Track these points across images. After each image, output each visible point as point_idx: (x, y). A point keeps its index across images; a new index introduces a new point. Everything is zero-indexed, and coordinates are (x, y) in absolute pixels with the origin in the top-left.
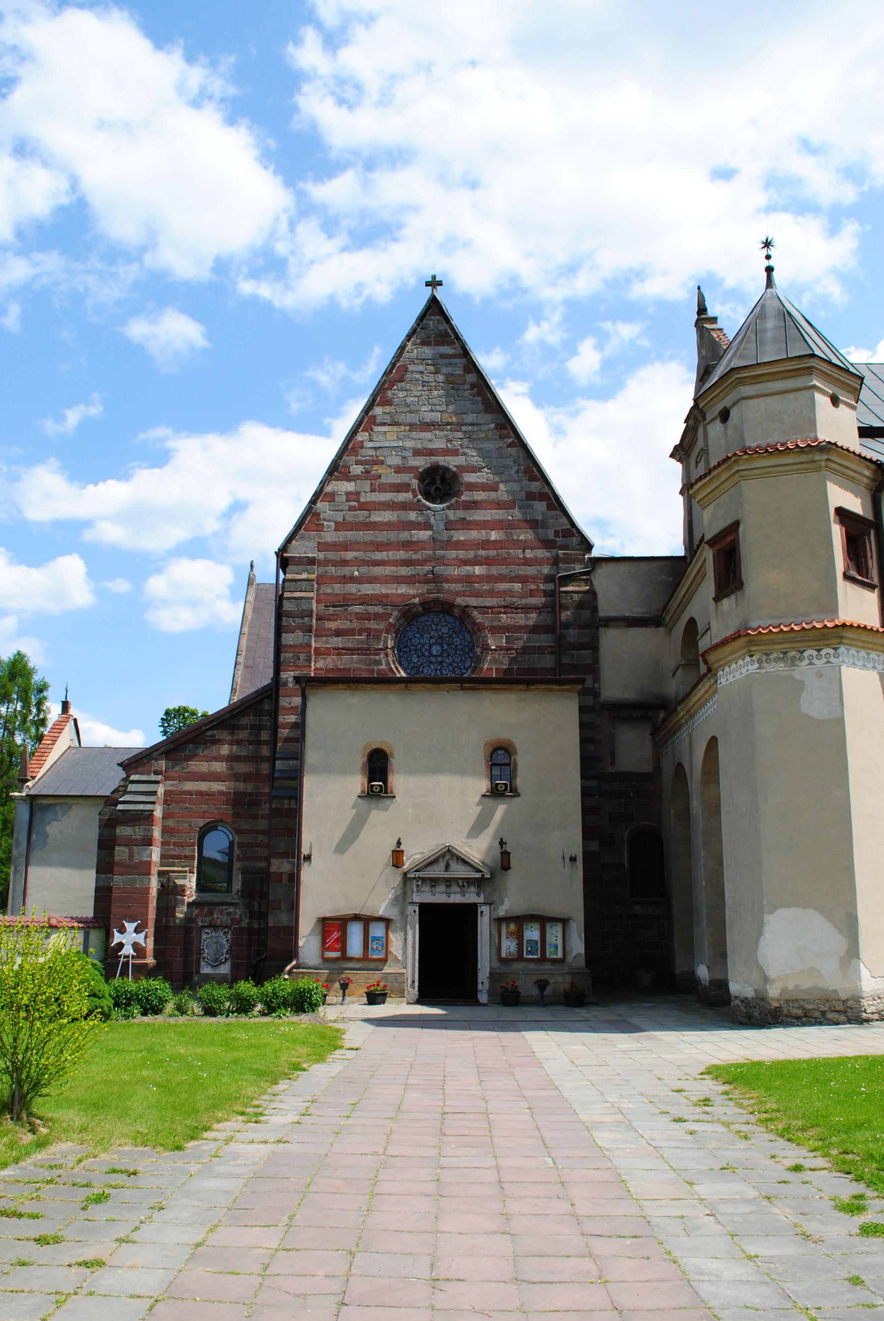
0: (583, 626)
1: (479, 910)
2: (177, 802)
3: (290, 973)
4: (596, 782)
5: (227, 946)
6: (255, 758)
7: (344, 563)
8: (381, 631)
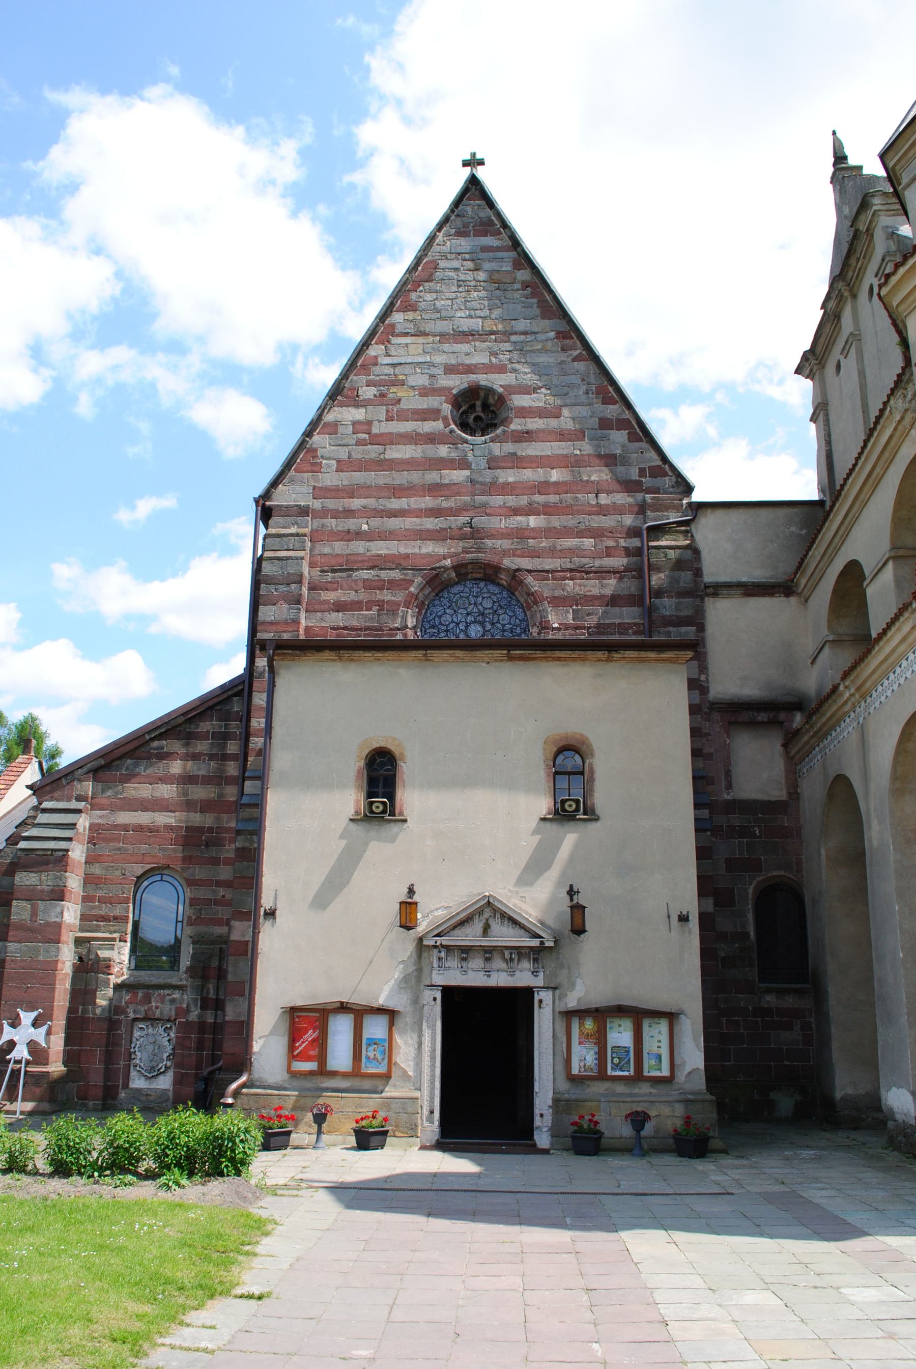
0: (681, 594)
1: (537, 998)
2: (107, 840)
3: (236, 1094)
4: (707, 811)
5: (169, 1049)
6: (219, 779)
7: (349, 513)
8: (398, 604)
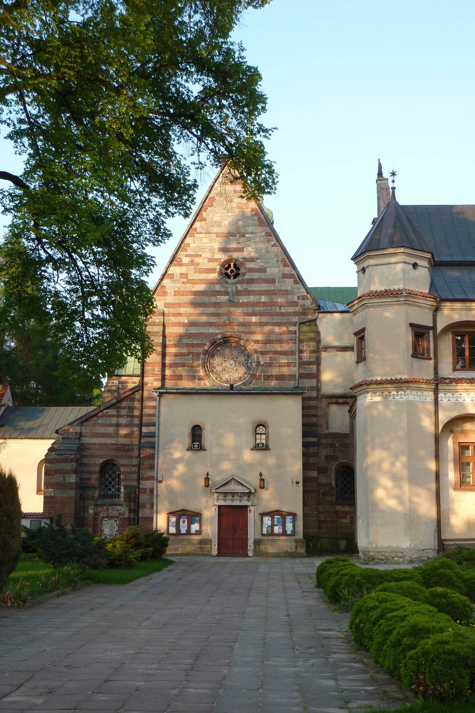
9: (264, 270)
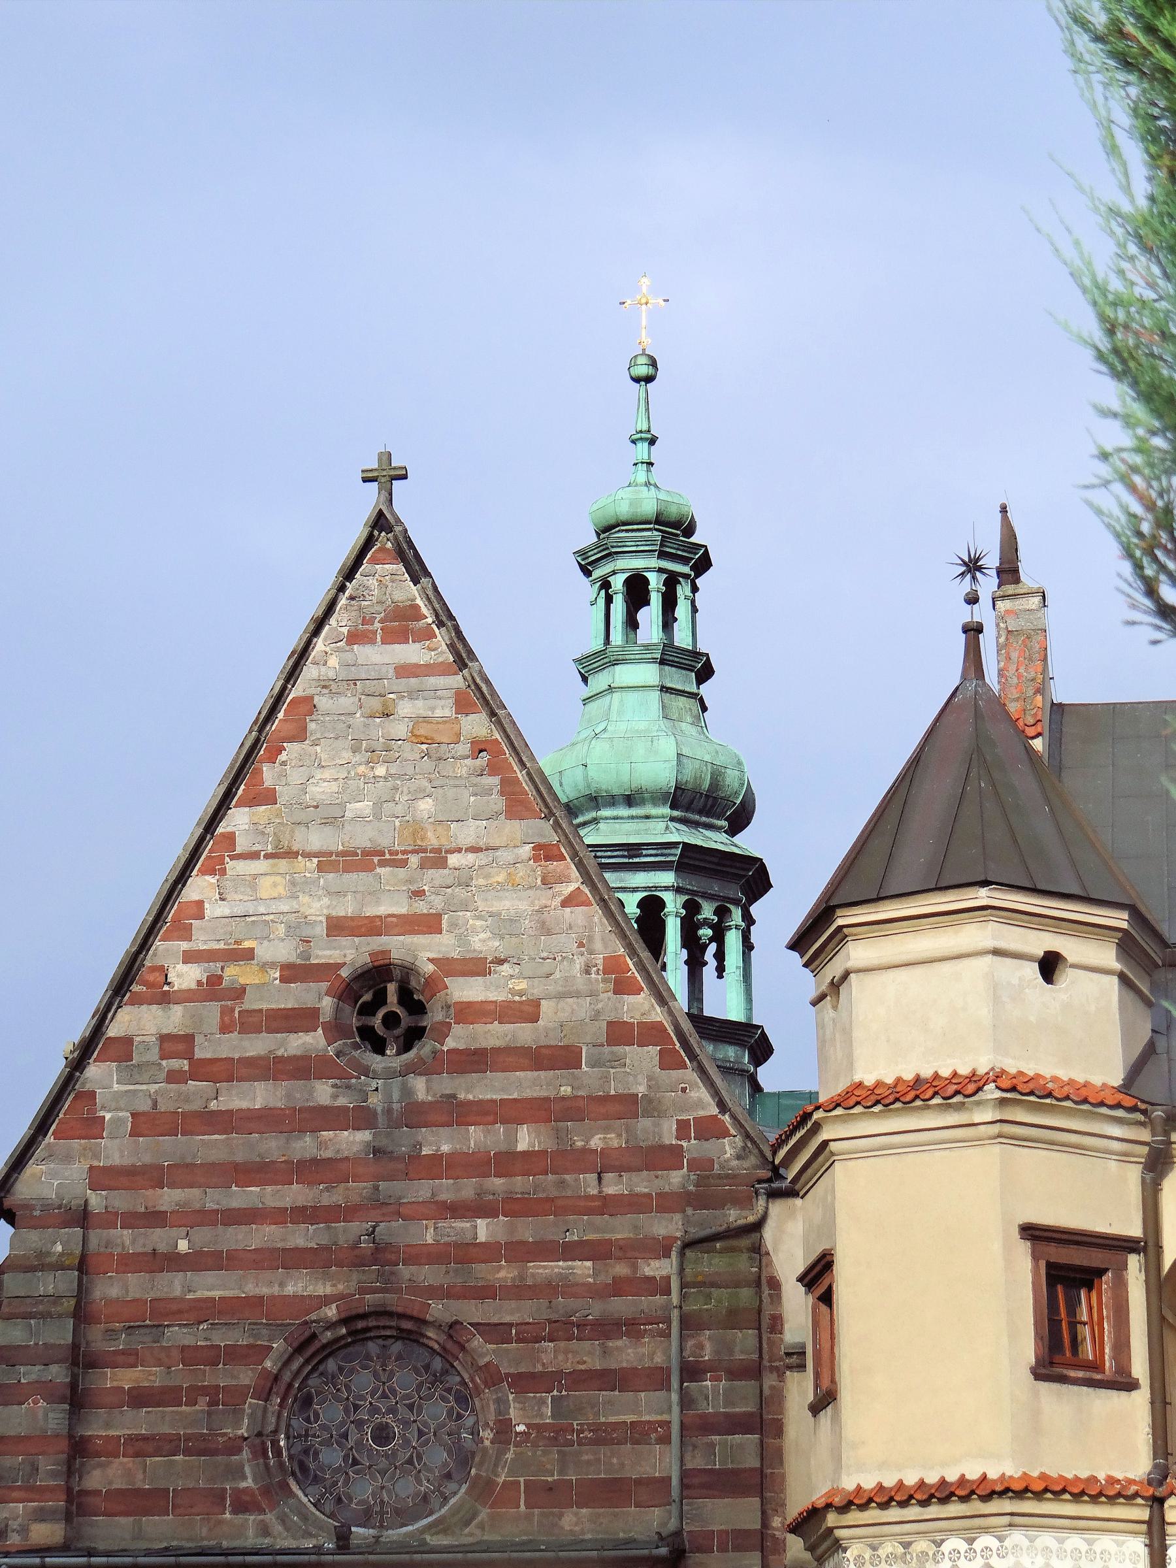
7: (155, 1218)
8: (239, 1394)
9: (528, 1011)
